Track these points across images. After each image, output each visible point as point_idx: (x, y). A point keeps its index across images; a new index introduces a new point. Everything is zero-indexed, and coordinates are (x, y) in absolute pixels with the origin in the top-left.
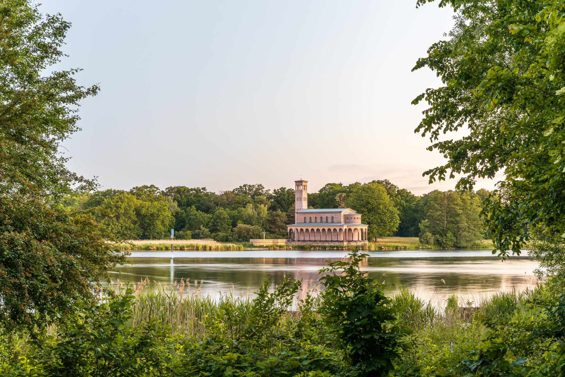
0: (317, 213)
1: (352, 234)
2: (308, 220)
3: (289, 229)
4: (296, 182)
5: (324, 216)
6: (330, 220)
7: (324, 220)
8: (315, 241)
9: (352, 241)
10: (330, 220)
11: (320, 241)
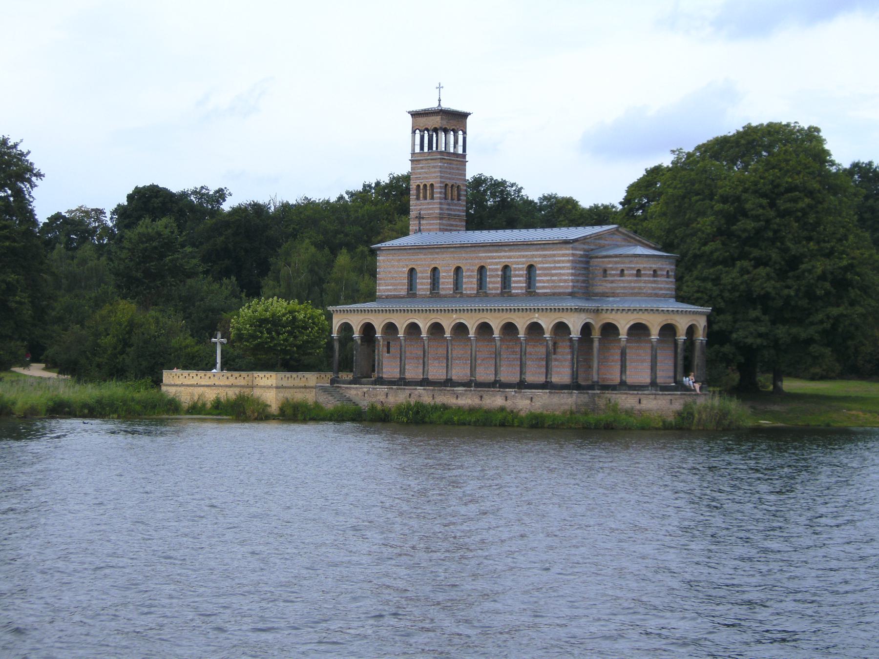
0: (463, 247)
1: (623, 354)
2: (423, 285)
3: (337, 323)
4: (415, 115)
5: (494, 263)
6: (518, 284)
7: (494, 283)
8: (449, 383)
9: (623, 386)
10: (518, 284)
11: (467, 384)
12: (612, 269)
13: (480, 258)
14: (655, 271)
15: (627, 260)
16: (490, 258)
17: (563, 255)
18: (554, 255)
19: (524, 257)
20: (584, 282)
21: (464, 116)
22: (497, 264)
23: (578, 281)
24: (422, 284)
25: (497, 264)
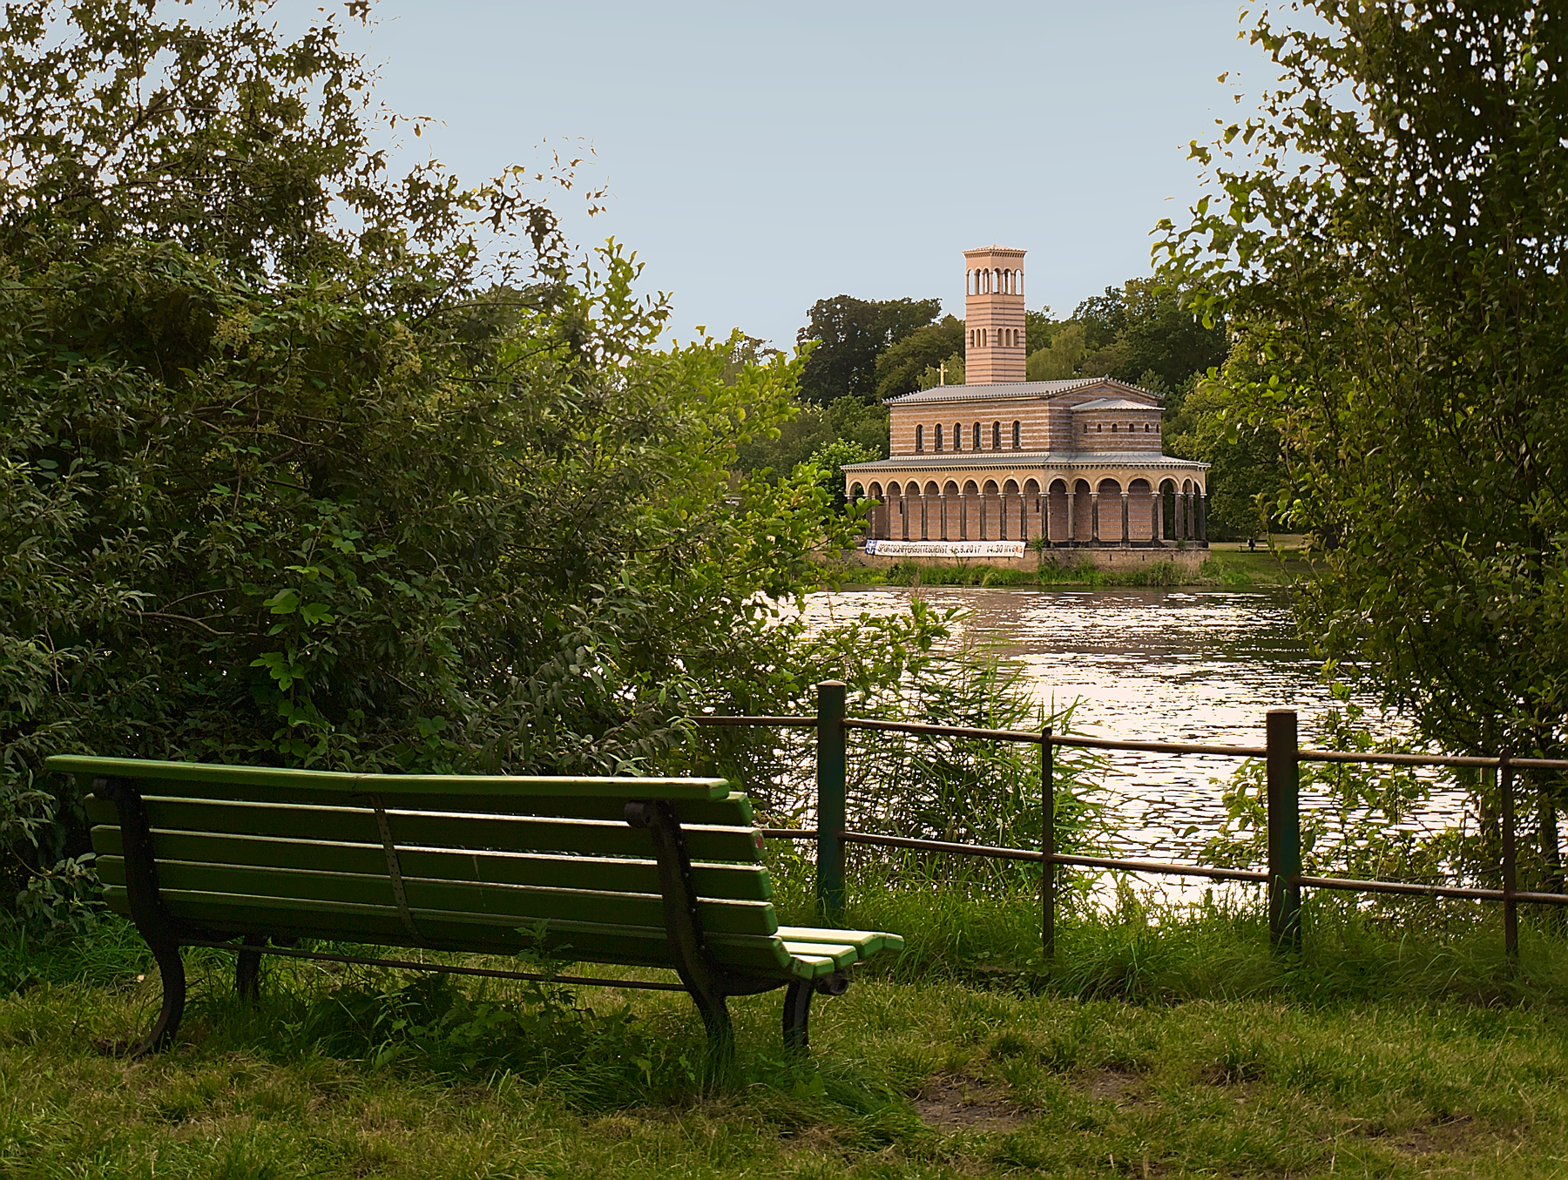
1: (1095, 510)
12: (1091, 424)
13: (975, 414)
14: (1132, 425)
15: (1103, 415)
16: (983, 414)
17: (1042, 411)
18: (1035, 412)
19: (1010, 413)
20: (1065, 437)
21: (1021, 255)
22: (989, 420)
23: (1057, 437)
24: (927, 441)
25: (989, 420)
